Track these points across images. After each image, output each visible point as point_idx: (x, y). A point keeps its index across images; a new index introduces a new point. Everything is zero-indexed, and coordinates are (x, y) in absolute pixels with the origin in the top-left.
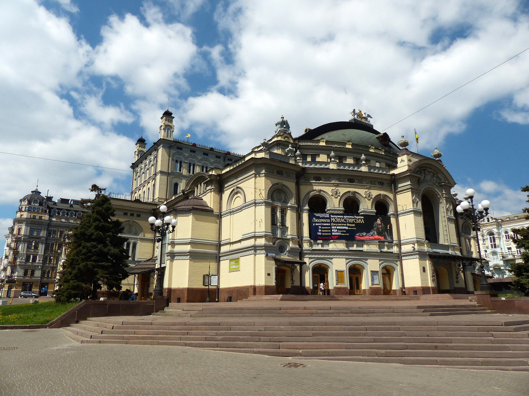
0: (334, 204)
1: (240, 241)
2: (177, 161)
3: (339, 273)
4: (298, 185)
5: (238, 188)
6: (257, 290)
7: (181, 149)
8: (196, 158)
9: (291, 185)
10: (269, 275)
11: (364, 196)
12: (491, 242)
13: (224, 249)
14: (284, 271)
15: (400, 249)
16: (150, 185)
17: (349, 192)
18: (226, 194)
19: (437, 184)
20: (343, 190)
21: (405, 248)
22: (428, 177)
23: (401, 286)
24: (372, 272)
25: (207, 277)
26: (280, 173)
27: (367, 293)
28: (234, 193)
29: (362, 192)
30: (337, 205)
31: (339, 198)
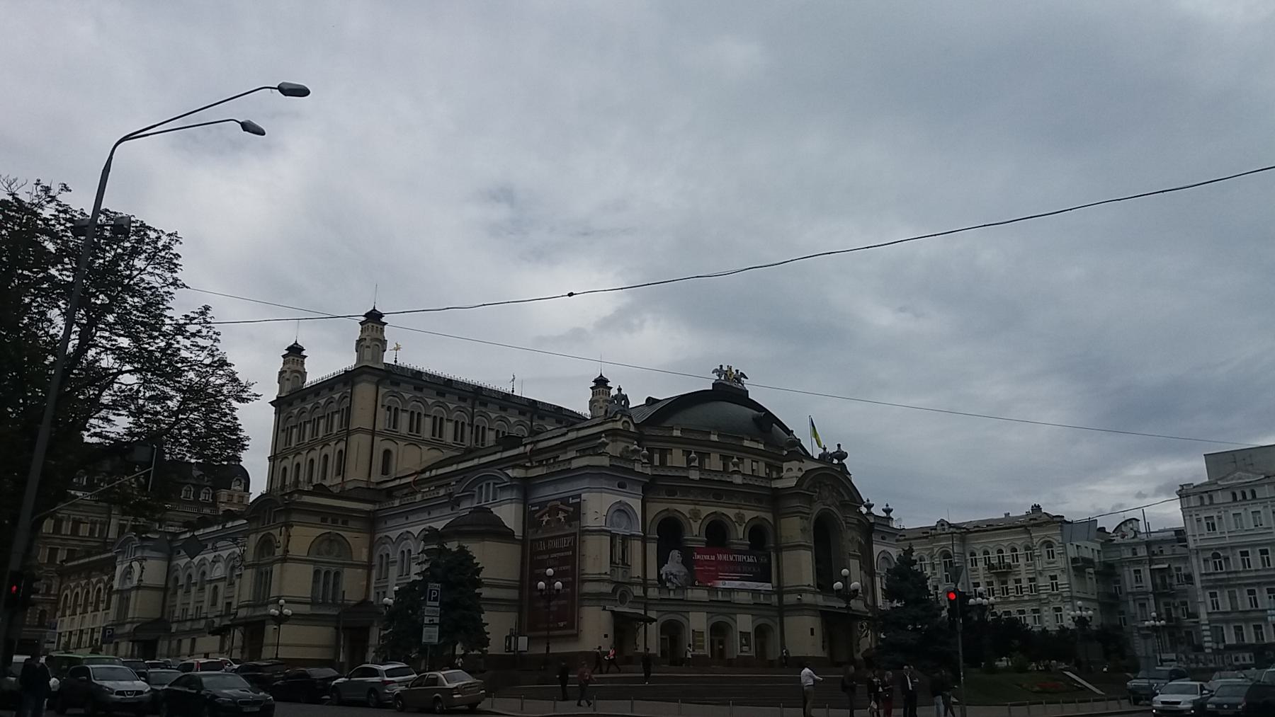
0: (695, 531)
2: (389, 408)
7: (398, 384)
8: (425, 403)
9: (636, 504)
10: (606, 636)
15: (781, 599)
16: (332, 450)
20: (705, 511)
21: (790, 599)
26: (621, 486)
29: (731, 513)
30: (696, 532)
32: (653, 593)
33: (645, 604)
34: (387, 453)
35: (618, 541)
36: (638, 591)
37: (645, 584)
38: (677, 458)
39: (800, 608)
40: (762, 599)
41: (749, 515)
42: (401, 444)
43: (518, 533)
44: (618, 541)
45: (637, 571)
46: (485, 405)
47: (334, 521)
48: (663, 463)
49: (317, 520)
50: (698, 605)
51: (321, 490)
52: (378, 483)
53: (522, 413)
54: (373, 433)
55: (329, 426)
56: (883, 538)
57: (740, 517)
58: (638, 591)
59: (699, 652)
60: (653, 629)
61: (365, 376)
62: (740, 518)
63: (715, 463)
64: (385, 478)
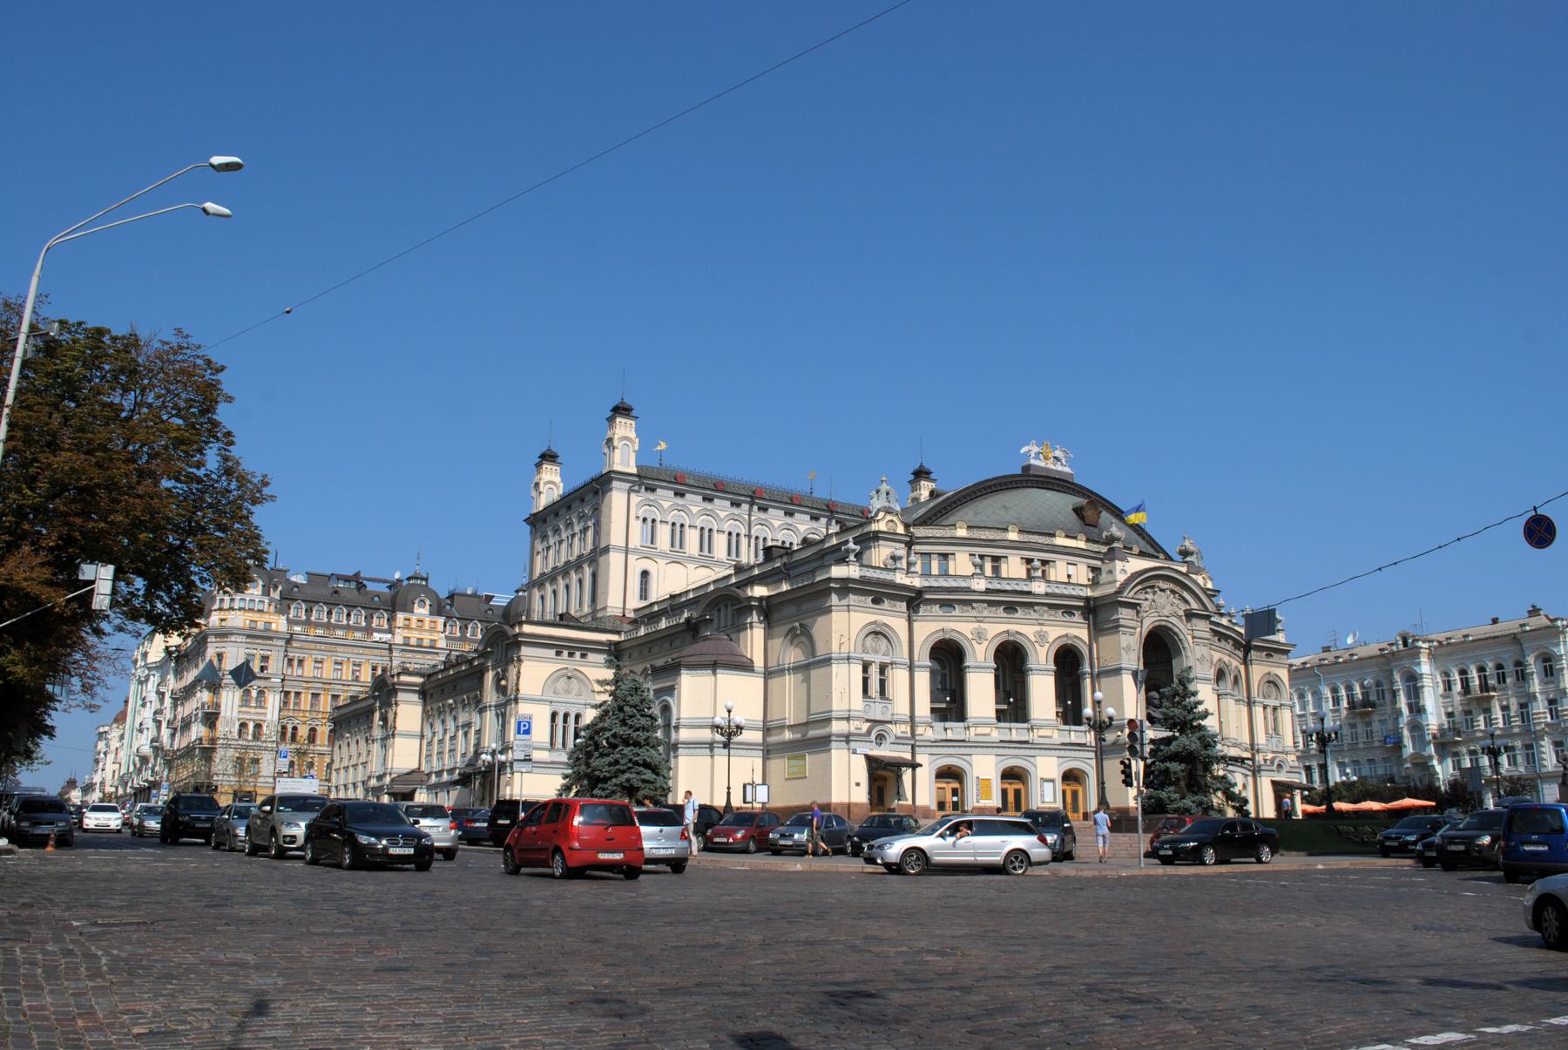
3: (984, 785)
9: (898, 624)
14: (885, 779)
19: (1181, 613)
22: (1161, 599)
33: (913, 747)
34: (645, 574)
35: (874, 671)
36: (902, 730)
38: (962, 563)
42: (662, 562)
43: (759, 662)
44: (874, 671)
45: (901, 707)
46: (764, 509)
47: (571, 655)
48: (945, 574)
49: (552, 653)
51: (564, 620)
52: (636, 611)
53: (815, 518)
54: (627, 551)
56: (1269, 655)
57: (1042, 637)
58: (902, 730)
59: (984, 803)
60: (925, 775)
63: (1014, 567)
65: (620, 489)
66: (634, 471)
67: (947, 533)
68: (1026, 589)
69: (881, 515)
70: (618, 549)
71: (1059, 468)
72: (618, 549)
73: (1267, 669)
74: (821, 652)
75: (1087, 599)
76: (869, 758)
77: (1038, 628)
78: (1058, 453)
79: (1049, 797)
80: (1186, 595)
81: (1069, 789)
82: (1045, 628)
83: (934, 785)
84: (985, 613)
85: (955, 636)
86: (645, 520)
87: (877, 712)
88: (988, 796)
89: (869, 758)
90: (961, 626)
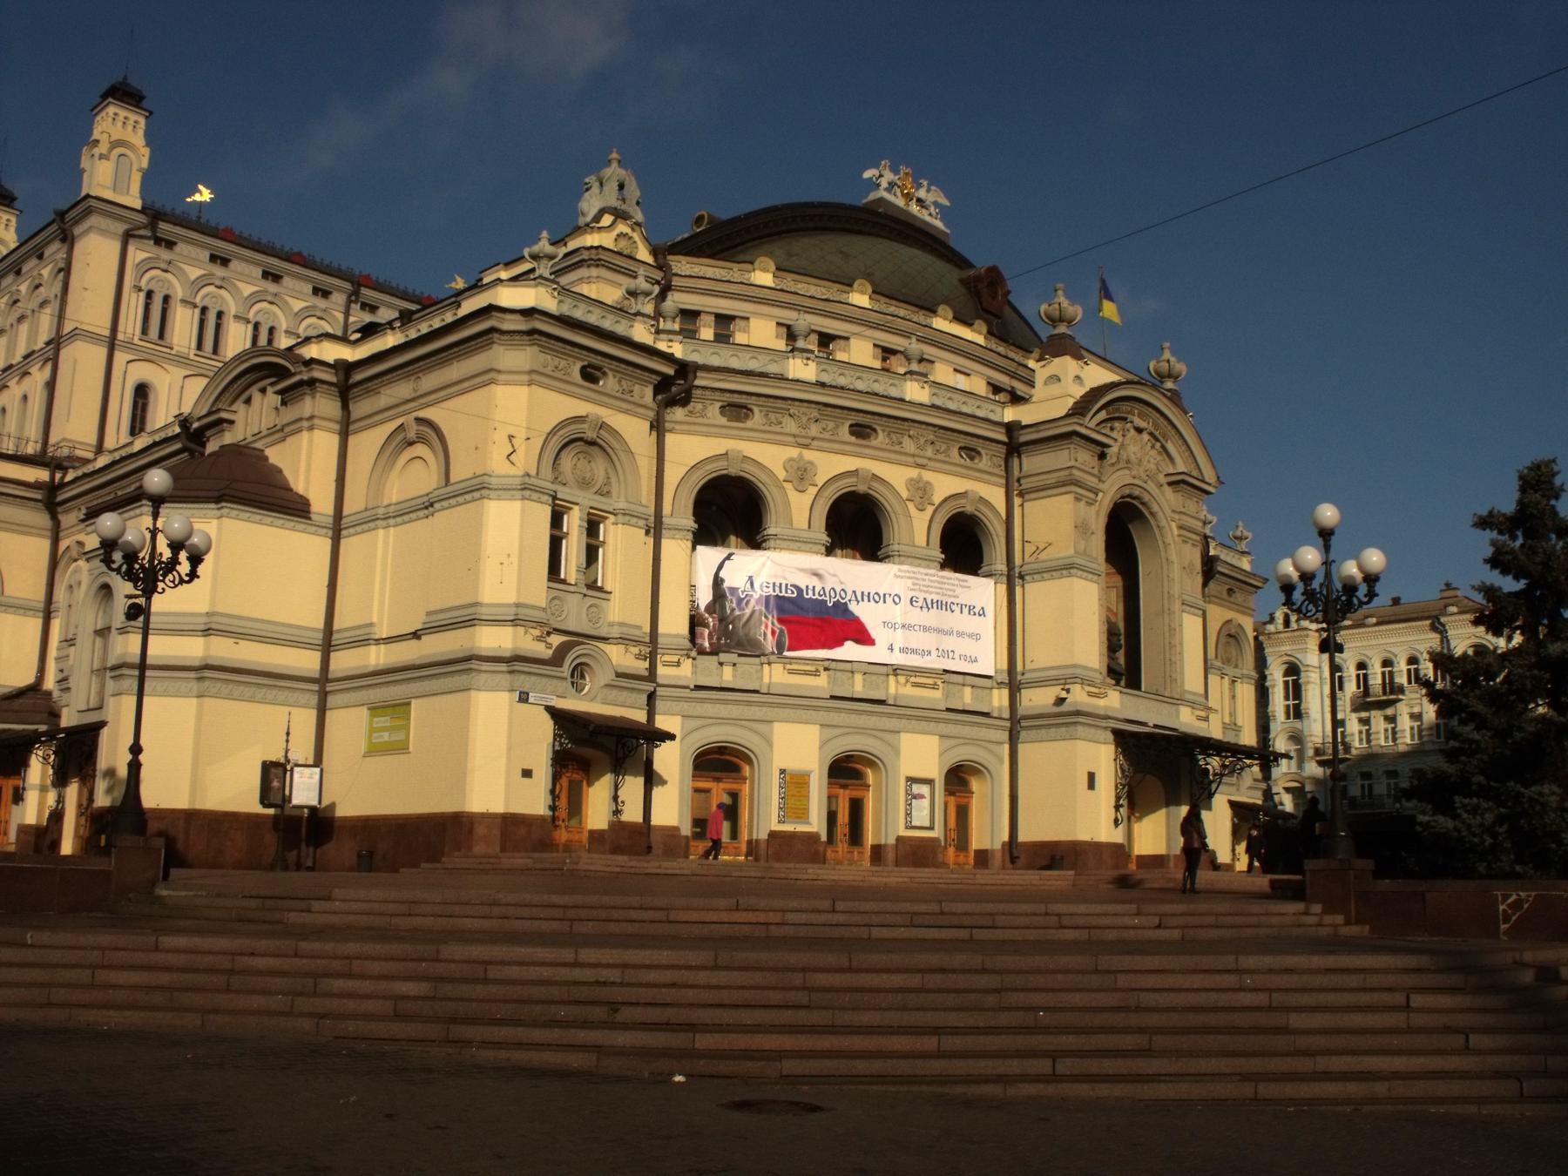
1: (416, 635)
3: (794, 783)
4: (658, 427)
5: (419, 420)
6: (480, 830)
7: (170, 245)
9: (633, 430)
10: (527, 773)
11: (905, 494)
12: (1287, 698)
13: (343, 662)
17: (855, 473)
18: (367, 444)
19: (1162, 479)
23: (1006, 837)
24: (912, 780)
25: (274, 774)
27: (890, 856)
28: (400, 442)
30: (800, 516)
31: (813, 490)
32: (677, 671)
33: (651, 697)
34: (142, 391)
35: (574, 523)
37: (652, 645)
39: (1064, 718)
40: (967, 698)
41: (945, 485)
50: (796, 703)
54: (112, 344)
55: (33, 334)
61: (94, 220)
62: (921, 492)
64: (140, 443)
65: (105, 232)
66: (138, 204)
67: (732, 272)
68: (894, 392)
69: (607, 220)
70: (92, 337)
71: (928, 219)
72: (92, 337)
73: (1230, 615)
74: (461, 471)
75: (1012, 428)
76: (556, 714)
77: (913, 473)
78: (922, 193)
79: (921, 814)
80: (1170, 446)
81: (952, 799)
82: (928, 476)
83: (689, 783)
84: (814, 430)
85: (751, 473)
86: (149, 294)
87: (575, 614)
88: (802, 814)
89: (556, 714)
90: (764, 455)
